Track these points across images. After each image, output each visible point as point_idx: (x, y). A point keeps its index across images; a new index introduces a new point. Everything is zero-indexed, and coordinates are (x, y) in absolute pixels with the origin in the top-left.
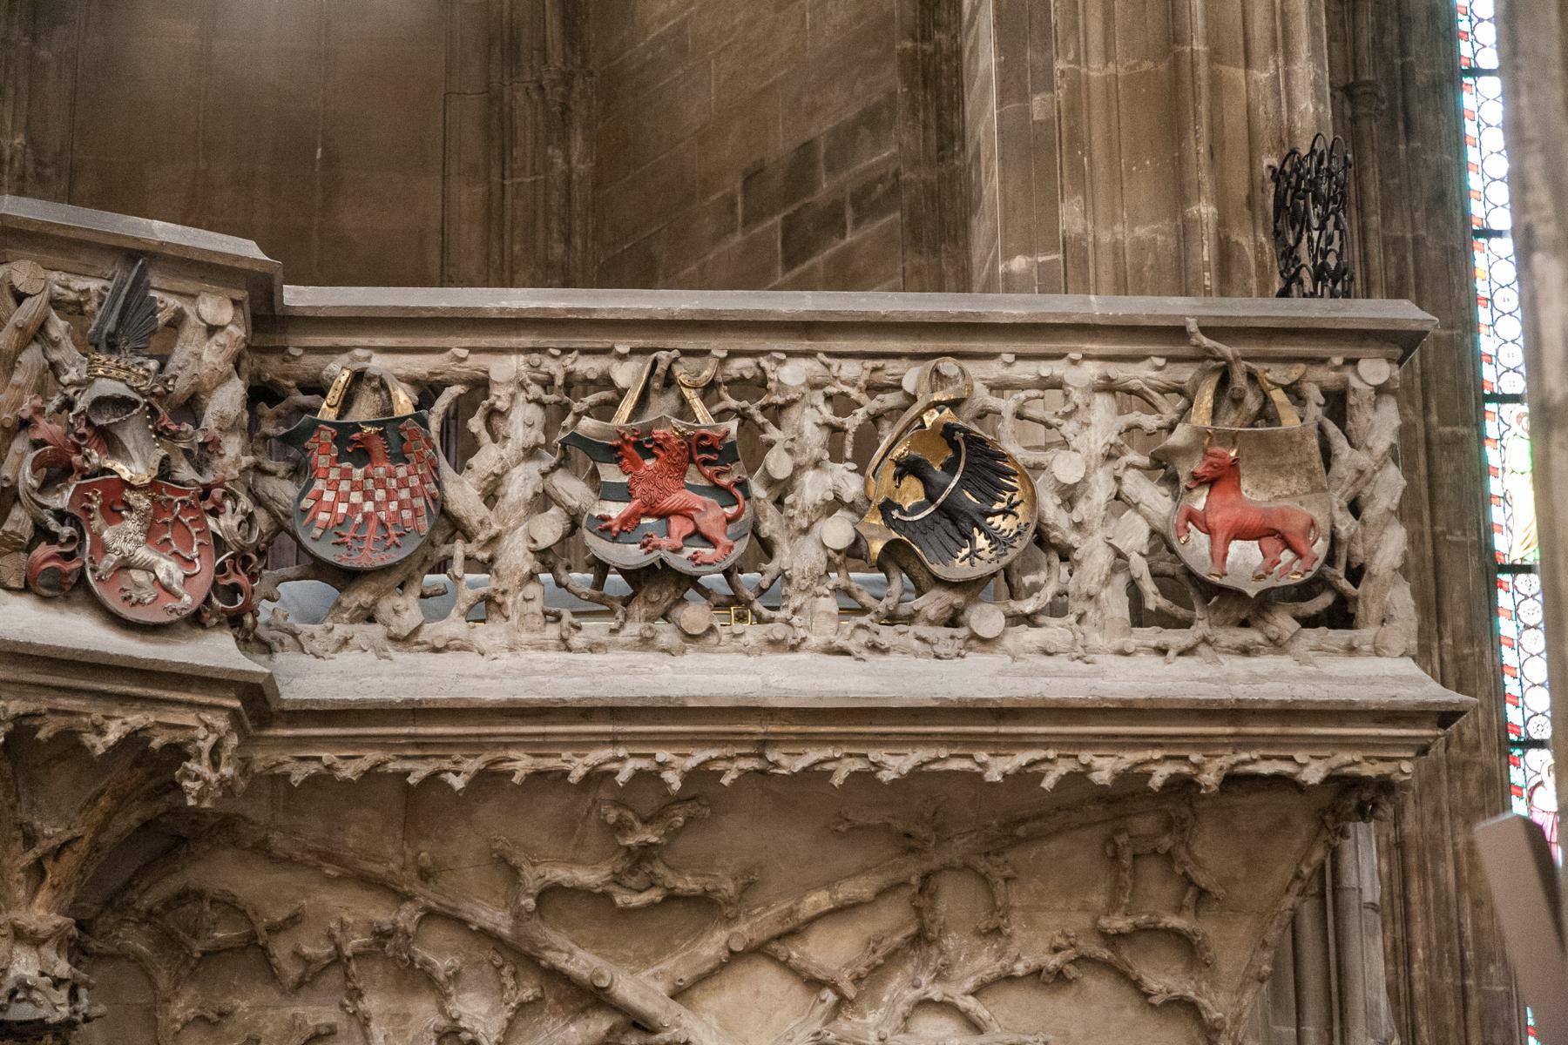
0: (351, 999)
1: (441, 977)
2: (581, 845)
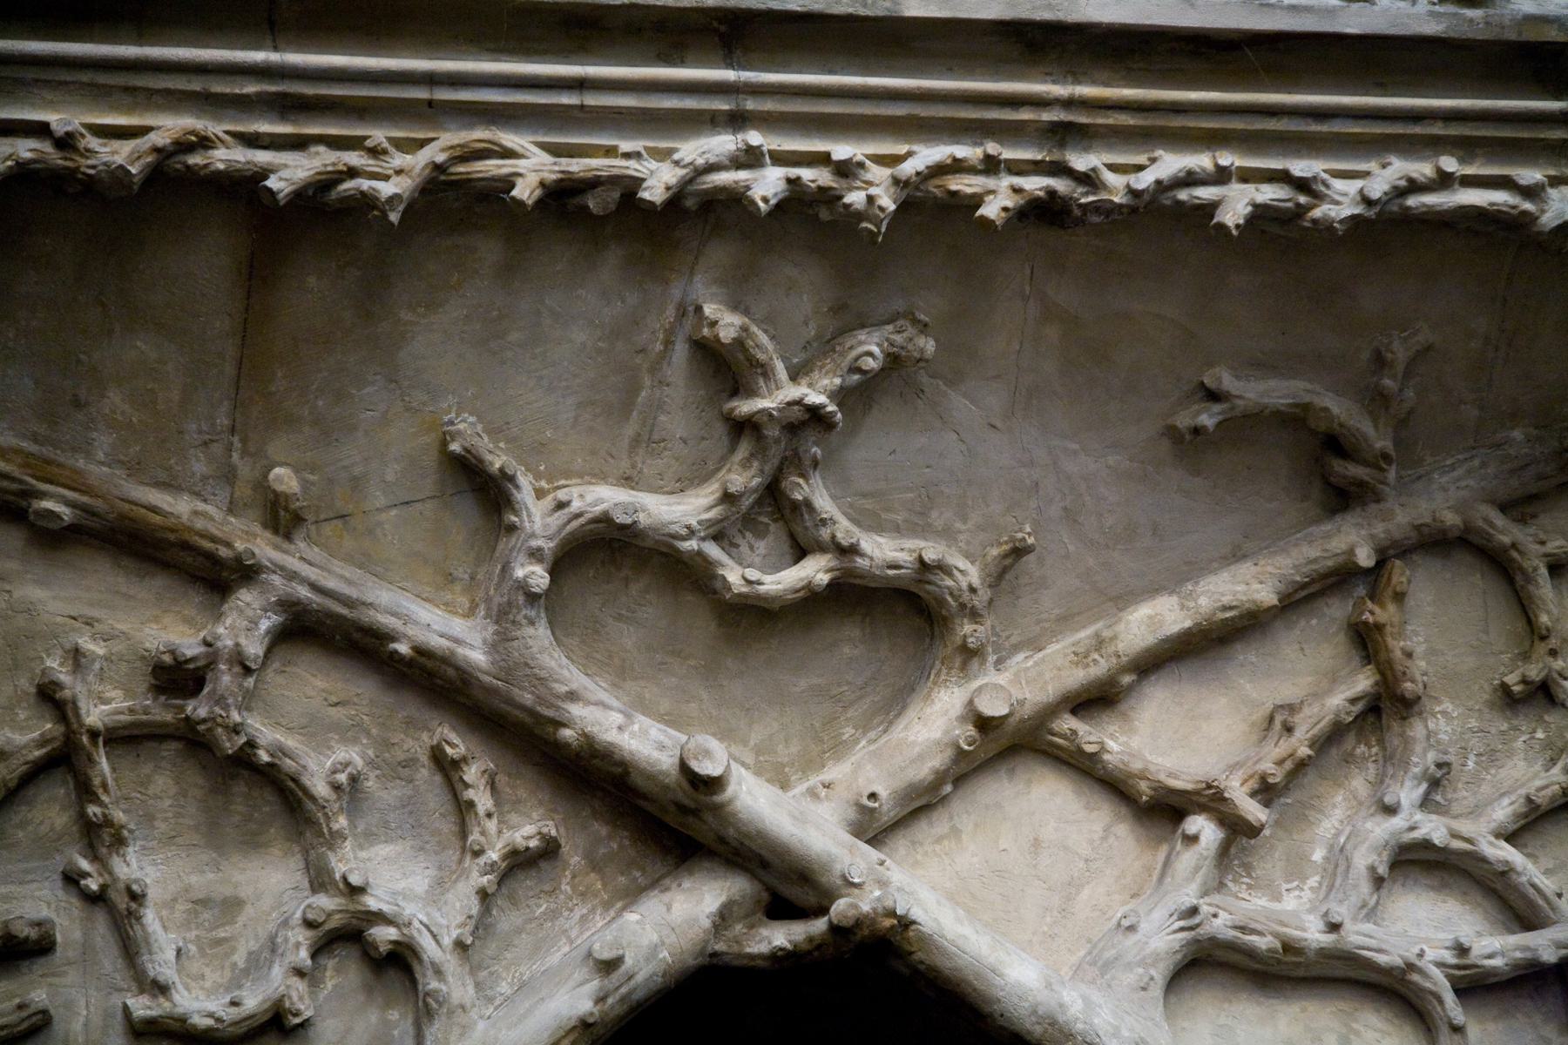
0: (95, 858)
1: (321, 789)
2: (649, 441)
